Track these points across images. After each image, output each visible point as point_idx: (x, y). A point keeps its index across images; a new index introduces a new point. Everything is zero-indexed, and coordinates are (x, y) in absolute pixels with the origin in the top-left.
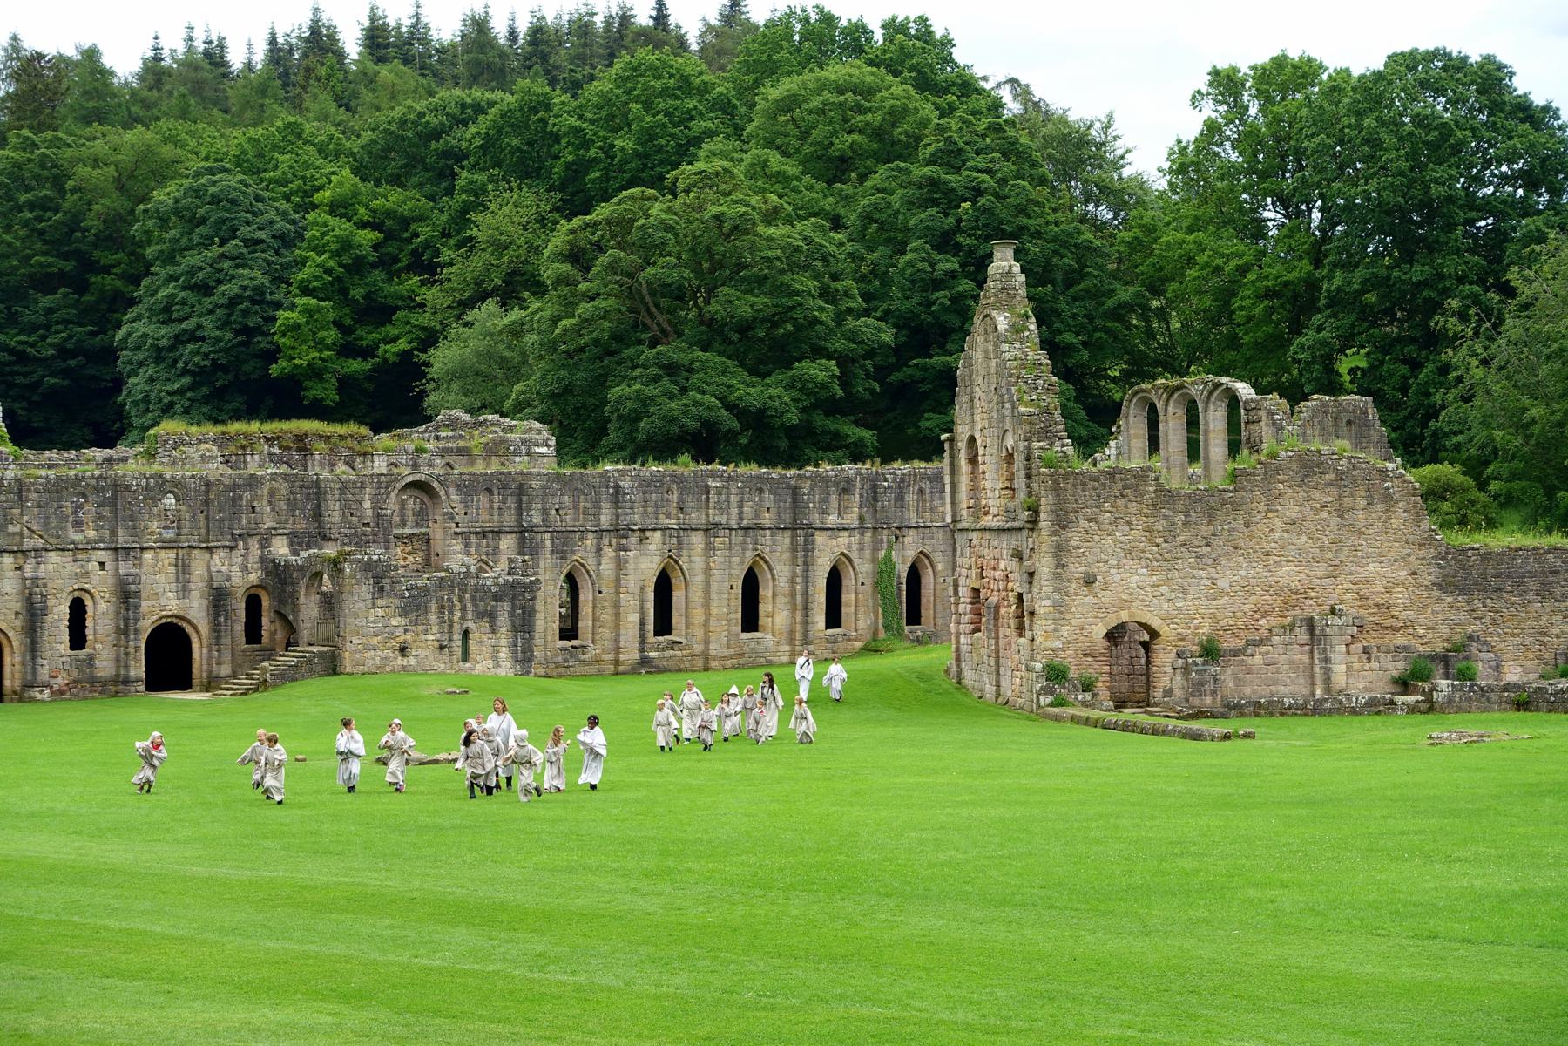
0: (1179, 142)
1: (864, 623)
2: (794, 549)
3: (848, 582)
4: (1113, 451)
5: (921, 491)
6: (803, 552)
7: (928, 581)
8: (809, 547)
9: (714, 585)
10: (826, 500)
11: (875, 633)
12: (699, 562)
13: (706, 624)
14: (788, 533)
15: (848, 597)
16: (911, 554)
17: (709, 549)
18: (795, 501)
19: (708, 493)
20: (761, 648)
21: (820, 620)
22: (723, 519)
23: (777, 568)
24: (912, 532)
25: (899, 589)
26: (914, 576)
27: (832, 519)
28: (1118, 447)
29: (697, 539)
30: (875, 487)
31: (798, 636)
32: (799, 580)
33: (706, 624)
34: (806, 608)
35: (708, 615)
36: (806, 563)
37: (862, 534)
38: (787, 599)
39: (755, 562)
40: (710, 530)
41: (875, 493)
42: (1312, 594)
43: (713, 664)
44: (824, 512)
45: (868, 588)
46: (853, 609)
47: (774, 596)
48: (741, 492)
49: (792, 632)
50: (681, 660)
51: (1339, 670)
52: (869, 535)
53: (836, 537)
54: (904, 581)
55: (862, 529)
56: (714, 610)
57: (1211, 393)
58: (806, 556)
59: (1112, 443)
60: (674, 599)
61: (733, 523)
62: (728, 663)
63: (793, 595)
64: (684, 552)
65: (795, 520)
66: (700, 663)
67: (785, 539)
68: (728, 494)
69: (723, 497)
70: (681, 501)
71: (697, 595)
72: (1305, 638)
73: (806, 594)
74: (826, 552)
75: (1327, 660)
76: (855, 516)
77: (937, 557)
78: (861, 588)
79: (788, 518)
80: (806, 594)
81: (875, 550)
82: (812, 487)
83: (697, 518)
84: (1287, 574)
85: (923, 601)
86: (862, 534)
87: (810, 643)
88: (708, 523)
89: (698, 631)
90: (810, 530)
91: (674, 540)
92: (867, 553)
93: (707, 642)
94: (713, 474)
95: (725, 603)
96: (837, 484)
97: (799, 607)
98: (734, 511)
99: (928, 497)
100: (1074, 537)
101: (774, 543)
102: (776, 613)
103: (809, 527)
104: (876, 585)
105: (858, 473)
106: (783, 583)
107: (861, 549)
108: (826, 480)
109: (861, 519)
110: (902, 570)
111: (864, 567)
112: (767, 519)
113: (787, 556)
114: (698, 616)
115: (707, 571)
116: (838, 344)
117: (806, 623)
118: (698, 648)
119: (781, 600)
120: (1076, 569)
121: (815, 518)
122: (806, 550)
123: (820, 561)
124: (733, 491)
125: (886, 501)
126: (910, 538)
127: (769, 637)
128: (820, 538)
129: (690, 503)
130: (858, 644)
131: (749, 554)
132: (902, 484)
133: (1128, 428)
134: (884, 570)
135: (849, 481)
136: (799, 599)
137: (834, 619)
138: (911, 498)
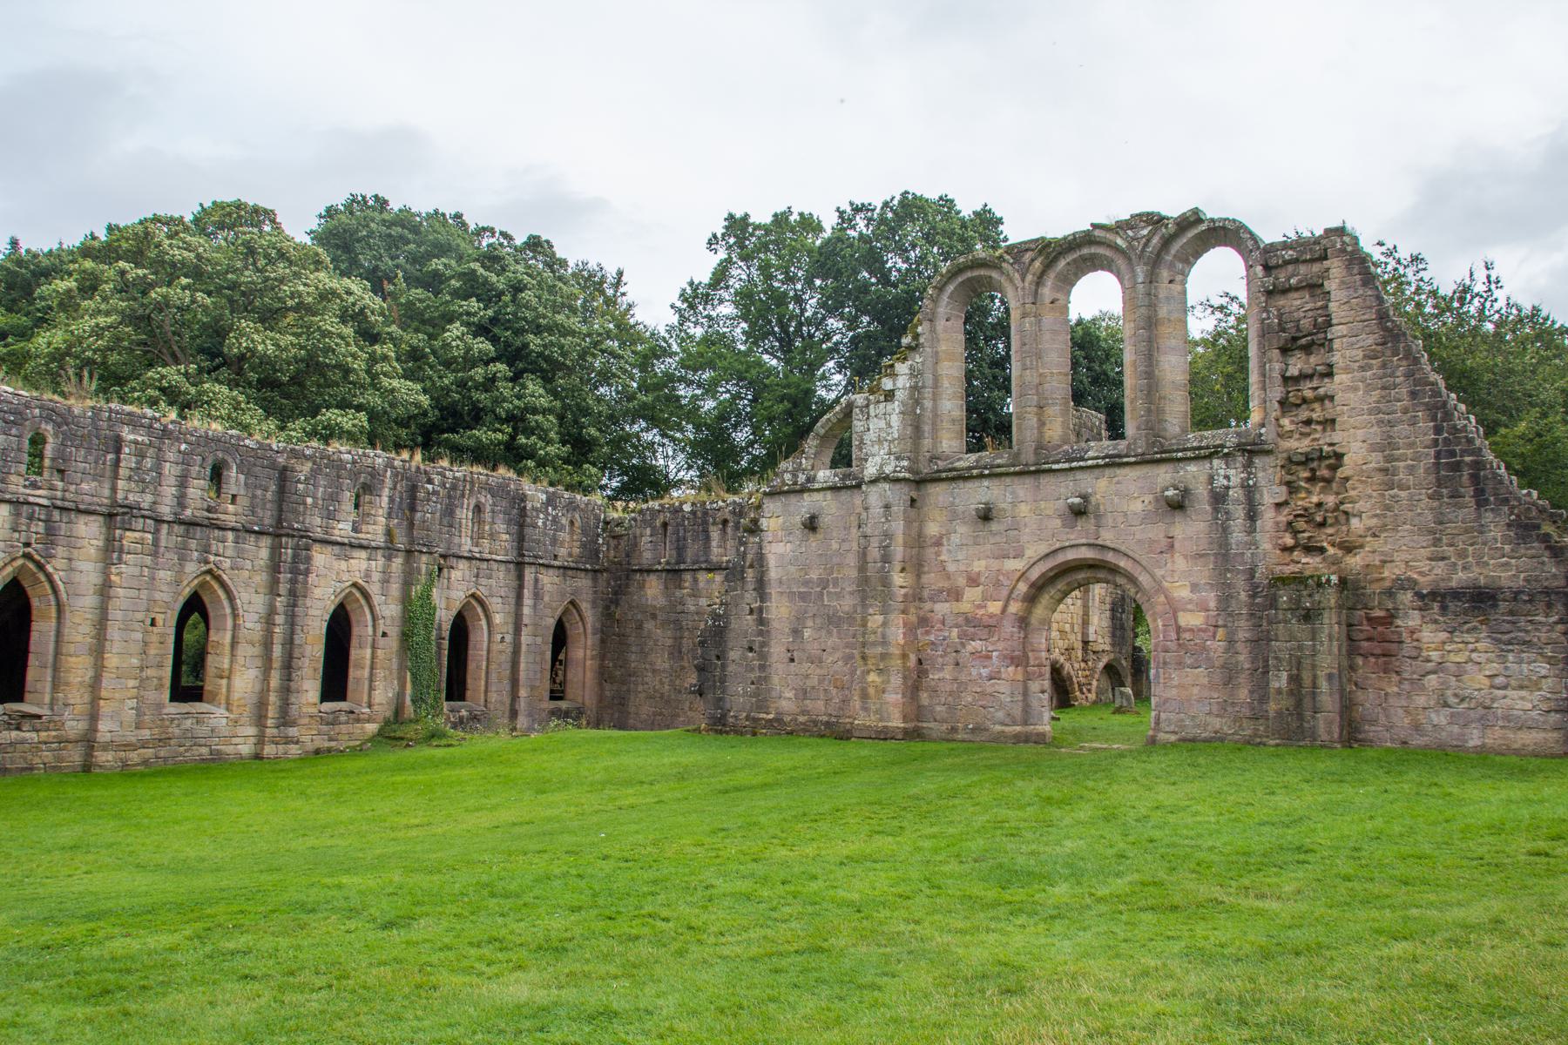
0: (691, 284)
1: (383, 694)
2: (274, 567)
3: (362, 630)
4: (903, 382)
5: (478, 509)
6: (289, 576)
7: (479, 638)
8: (300, 569)
9: (115, 614)
10: (334, 498)
11: (398, 711)
12: (88, 571)
13: (95, 685)
14: (266, 542)
15: (360, 654)
16: (459, 595)
17: (111, 551)
18: (281, 491)
19: (118, 451)
20: (202, 731)
21: (310, 688)
22: (146, 500)
23: (243, 597)
24: (463, 564)
25: (439, 646)
26: (460, 631)
27: (342, 529)
28: (914, 374)
29: (89, 531)
30: (413, 489)
31: (272, 712)
32: (280, 619)
33: (95, 685)
34: (288, 666)
35: (99, 668)
36: (293, 593)
37: (389, 558)
38: (257, 650)
39: (203, 585)
40: (116, 516)
41: (413, 498)
43: (104, 757)
44: (331, 516)
45: (392, 643)
46: (366, 673)
47: (234, 643)
48: (185, 460)
49: (262, 705)
50: (36, 748)
52: (398, 562)
53: (348, 558)
54: (446, 634)
55: (389, 549)
56: (112, 660)
57: (1167, 242)
58: (293, 581)
59: (902, 368)
60: (34, 636)
61: (166, 511)
62: (134, 757)
63: (267, 644)
64: (60, 551)
65: (279, 521)
66: (75, 756)
67: (261, 551)
68: (160, 460)
69: (148, 463)
70: (61, 455)
71: (79, 630)
73: (289, 642)
74: (329, 578)
76: (380, 529)
77: (495, 604)
78: (381, 642)
79: (267, 517)
80: (289, 642)
81: (407, 584)
82: (315, 473)
83: (90, 490)
85: (471, 666)
86: (389, 558)
87: (293, 724)
88: (114, 504)
89: (77, 698)
90: (305, 540)
91: (41, 527)
92: (395, 588)
93: (94, 717)
94: (134, 422)
95: (135, 648)
96: (355, 475)
97: (276, 664)
98: (169, 491)
99: (487, 516)
101: (240, 554)
102: (239, 675)
103: (304, 534)
104: (405, 637)
105: (389, 464)
106: (251, 623)
107: (385, 581)
108: (338, 465)
109: (389, 533)
110: (445, 616)
111: (389, 610)
112: (231, 513)
113: (261, 578)
114: (78, 668)
115: (105, 590)
116: (374, 399)
117: (286, 691)
118: (74, 726)
119: (248, 652)
121: (315, 522)
122: (295, 571)
123: (317, 592)
124: (171, 456)
125: (429, 513)
126: (460, 573)
127: (222, 711)
128: (321, 558)
129: (80, 461)
130: (372, 728)
131: (192, 568)
132: (454, 494)
133: (935, 340)
134: (414, 615)
135: (374, 473)
136: (277, 651)
137: (335, 683)
138: (464, 514)
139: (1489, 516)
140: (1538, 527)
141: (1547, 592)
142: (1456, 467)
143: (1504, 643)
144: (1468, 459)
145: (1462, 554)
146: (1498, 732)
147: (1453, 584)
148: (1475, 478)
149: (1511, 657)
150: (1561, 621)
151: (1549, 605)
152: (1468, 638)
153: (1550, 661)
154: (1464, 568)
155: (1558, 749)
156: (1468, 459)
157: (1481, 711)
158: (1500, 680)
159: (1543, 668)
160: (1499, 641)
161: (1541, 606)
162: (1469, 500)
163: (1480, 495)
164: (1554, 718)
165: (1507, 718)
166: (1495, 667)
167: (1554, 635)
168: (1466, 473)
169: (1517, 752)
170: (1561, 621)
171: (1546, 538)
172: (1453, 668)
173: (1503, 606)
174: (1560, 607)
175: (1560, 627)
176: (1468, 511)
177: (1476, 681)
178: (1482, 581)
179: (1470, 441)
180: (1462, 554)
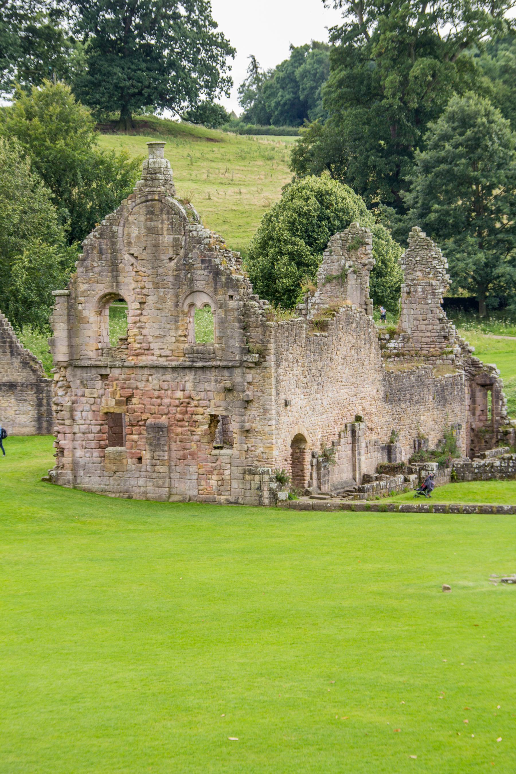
42: (349, 408)
51: (363, 458)
72: (350, 440)
75: (359, 454)
84: (344, 393)
100: (281, 371)
120: (283, 396)
139: (15, 359)
140: (29, 363)
141: (31, 384)
142: (5, 342)
143: (19, 400)
144: (8, 340)
145: (6, 371)
146: (17, 429)
147: (3, 381)
148: (10, 347)
149: (21, 405)
150: (35, 393)
151: (32, 388)
152: (8, 399)
153: (32, 406)
154: (7, 376)
155: (34, 433)
156: (8, 340)
157: (12, 422)
158: (18, 412)
159: (30, 408)
160: (17, 400)
161: (29, 388)
162: (8, 353)
163: (12, 351)
164: (34, 423)
165: (19, 424)
166: (16, 408)
167: (33, 398)
168: (8, 344)
169: (23, 435)
170: (35, 393)
171: (31, 367)
172: (3, 409)
173: (19, 388)
174: (35, 389)
175: (35, 395)
176: (8, 357)
177: (10, 413)
178: (12, 380)
179: (9, 334)
180: (6, 371)
